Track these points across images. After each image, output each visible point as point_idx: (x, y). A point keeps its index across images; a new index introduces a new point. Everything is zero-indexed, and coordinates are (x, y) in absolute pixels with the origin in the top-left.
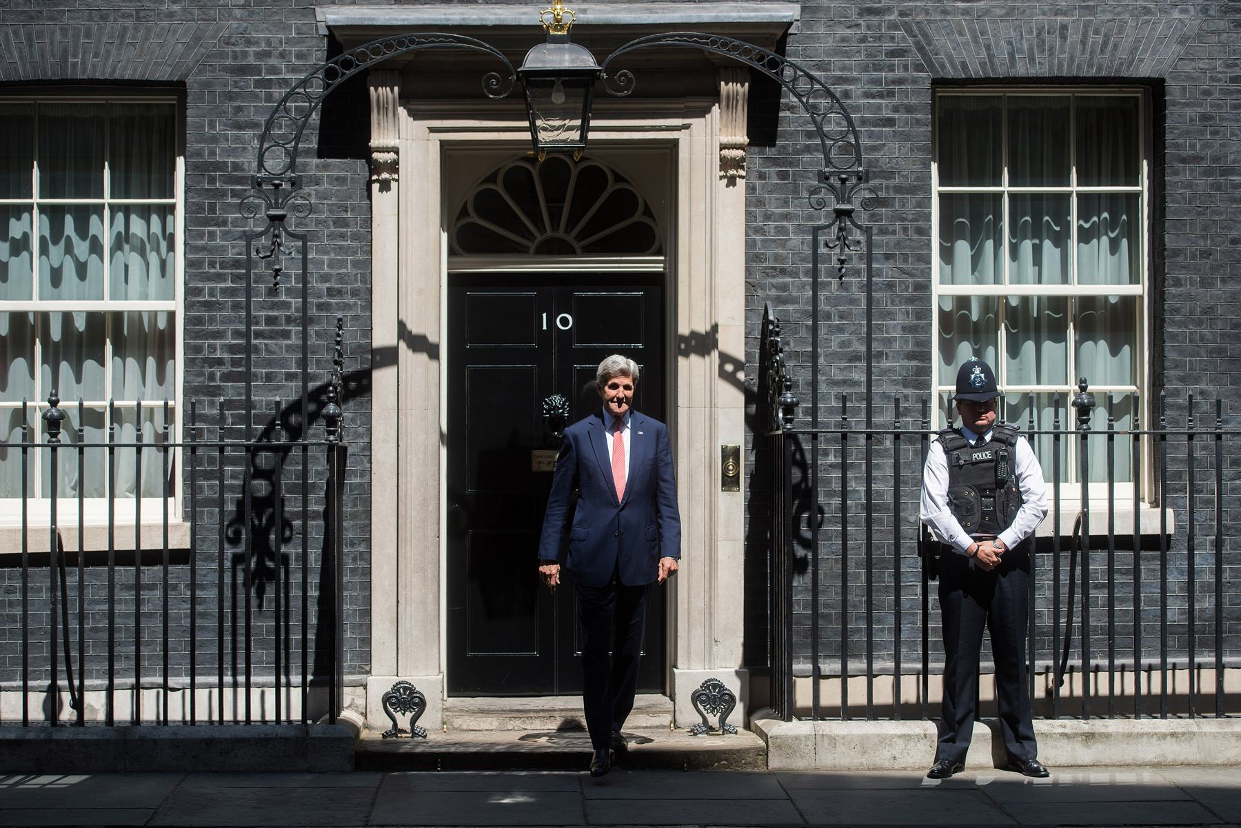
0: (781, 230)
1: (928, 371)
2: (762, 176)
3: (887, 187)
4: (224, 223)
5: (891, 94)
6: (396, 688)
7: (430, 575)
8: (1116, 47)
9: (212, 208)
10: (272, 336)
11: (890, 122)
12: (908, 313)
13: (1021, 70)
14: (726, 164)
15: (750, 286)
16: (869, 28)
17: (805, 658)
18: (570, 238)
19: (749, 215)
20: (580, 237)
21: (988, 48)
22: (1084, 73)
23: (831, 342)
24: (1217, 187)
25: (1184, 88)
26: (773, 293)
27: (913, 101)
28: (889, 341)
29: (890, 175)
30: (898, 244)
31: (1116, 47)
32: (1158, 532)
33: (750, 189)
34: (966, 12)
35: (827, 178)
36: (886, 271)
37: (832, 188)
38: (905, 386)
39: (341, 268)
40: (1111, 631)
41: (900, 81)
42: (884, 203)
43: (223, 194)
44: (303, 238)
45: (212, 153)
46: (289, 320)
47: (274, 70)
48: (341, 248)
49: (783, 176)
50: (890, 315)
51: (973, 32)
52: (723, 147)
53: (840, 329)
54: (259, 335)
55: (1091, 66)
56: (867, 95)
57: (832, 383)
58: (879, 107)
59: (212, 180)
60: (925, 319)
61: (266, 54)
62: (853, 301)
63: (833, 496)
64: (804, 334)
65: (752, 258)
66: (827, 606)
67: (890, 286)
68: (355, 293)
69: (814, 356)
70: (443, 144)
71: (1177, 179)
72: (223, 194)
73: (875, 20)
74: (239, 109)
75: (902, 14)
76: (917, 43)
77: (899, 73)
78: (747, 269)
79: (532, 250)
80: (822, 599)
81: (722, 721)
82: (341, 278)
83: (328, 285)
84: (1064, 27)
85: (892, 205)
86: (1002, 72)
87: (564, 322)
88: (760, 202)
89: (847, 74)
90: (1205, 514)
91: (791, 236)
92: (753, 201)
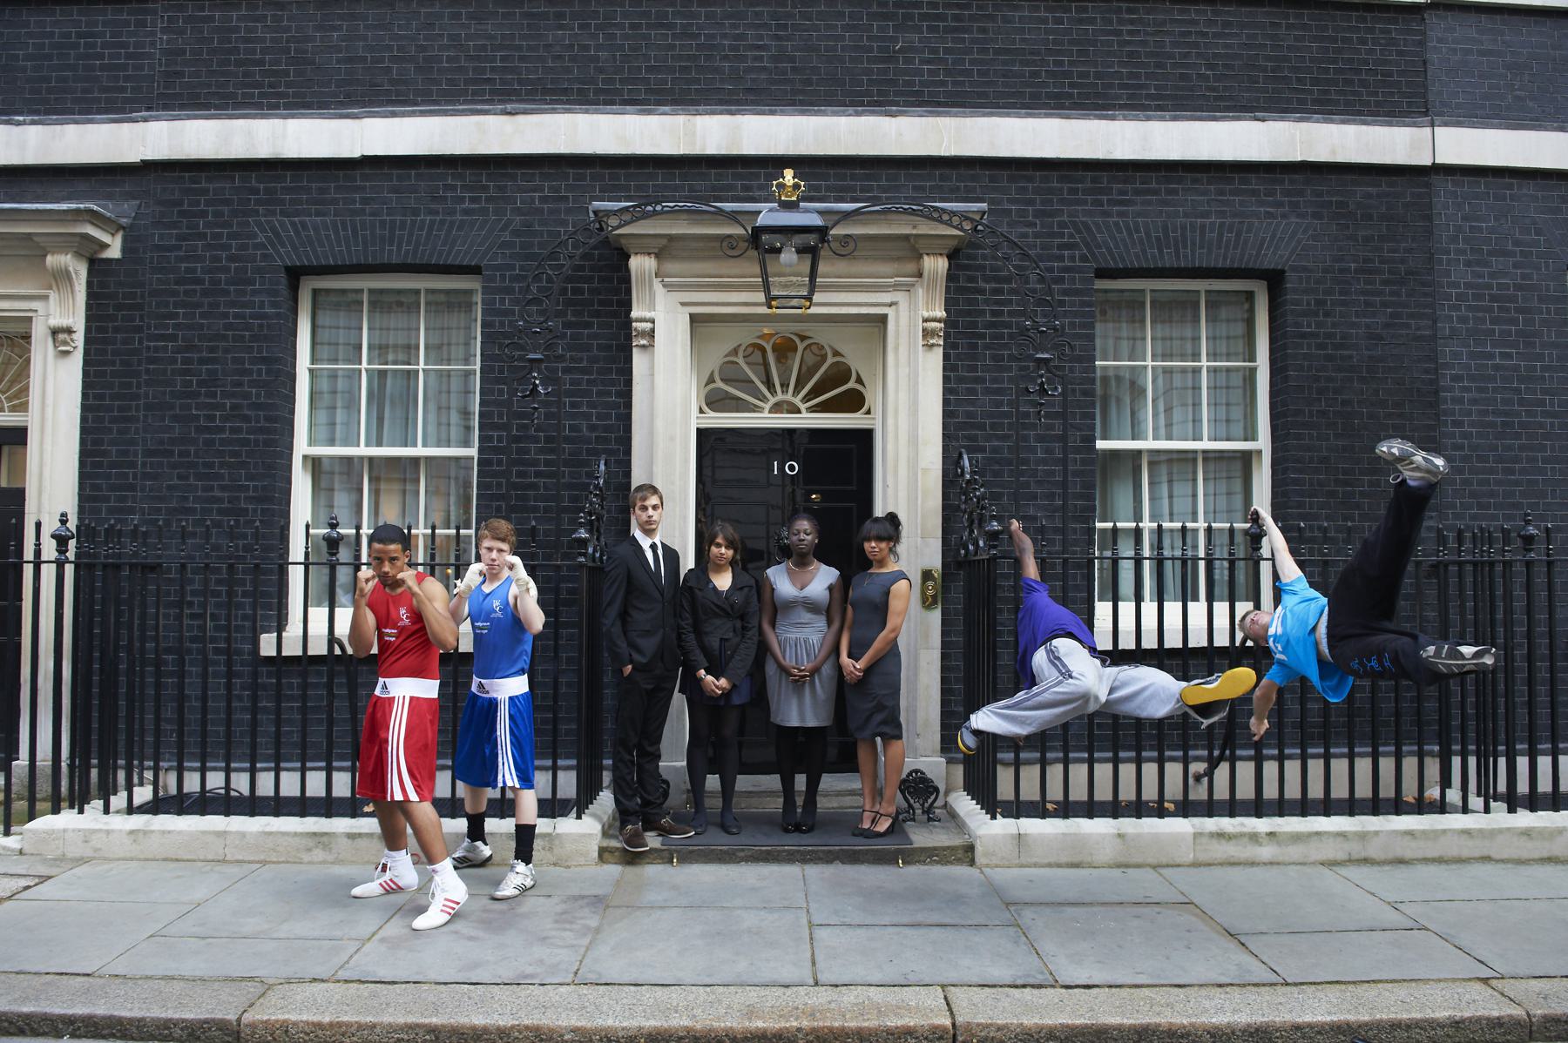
2: (955, 346)
14: (927, 333)
15: (946, 437)
16: (1042, 226)
18: (797, 401)
19: (946, 379)
20: (806, 399)
24: (1329, 358)
31: (1246, 242)
33: (946, 357)
52: (925, 320)
54: (538, 474)
55: (1225, 258)
65: (947, 414)
82: (607, 429)
84: (1203, 227)
87: (792, 468)
92: (947, 367)
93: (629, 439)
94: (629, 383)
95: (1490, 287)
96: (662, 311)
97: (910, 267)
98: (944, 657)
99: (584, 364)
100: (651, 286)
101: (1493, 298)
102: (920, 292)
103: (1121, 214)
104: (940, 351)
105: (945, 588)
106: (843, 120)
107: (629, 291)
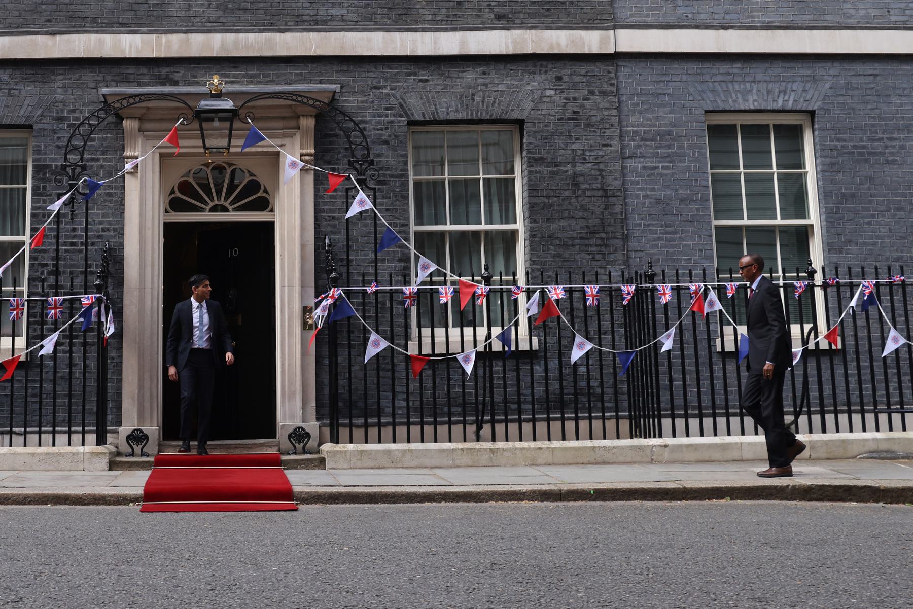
1: (409, 268)
4: (50, 195)
5: (387, 128)
8: (499, 104)
9: (44, 187)
10: (73, 252)
11: (387, 142)
13: (452, 116)
21: (435, 105)
22: (484, 117)
25: (534, 124)
26: (329, 228)
27: (399, 132)
29: (388, 169)
32: (528, 349)
34: (424, 88)
40: (505, 401)
41: (392, 122)
43: (49, 180)
45: (45, 160)
46: (82, 243)
47: (77, 119)
51: (427, 97)
53: (363, 247)
54: (66, 251)
56: (374, 129)
57: (358, 274)
58: (381, 135)
59: (45, 174)
61: (73, 111)
68: (115, 230)
69: (349, 261)
70: (162, 155)
71: (532, 169)
72: (49, 180)
73: (377, 92)
74: (59, 138)
75: (391, 89)
76: (400, 103)
77: (392, 118)
82: (110, 223)
86: (442, 118)
88: (322, 183)
89: (364, 119)
90: (552, 340)
95: (655, 125)
101: (658, 133)
103: (424, 88)
106: (251, 36)
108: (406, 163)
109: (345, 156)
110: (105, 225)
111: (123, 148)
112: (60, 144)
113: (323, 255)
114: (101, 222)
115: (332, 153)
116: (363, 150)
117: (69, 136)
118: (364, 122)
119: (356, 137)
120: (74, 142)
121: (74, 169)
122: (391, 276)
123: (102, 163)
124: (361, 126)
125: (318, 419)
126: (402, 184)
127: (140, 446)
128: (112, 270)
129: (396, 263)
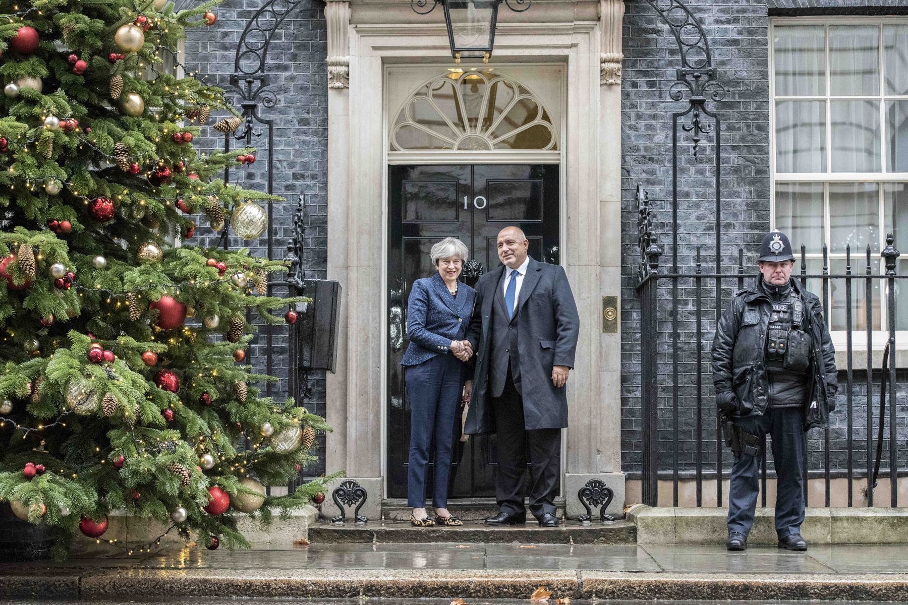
0: (649, 127)
2: (635, 85)
3: (734, 94)
5: (736, 20)
6: (344, 484)
7: (370, 396)
12: (751, 192)
15: (626, 171)
17: (670, 465)
23: (688, 218)
28: (735, 215)
30: (742, 139)
33: (625, 95)
35: (684, 75)
36: (732, 159)
37: (689, 84)
38: (749, 250)
39: (303, 157)
41: (744, 11)
42: (731, 106)
44: (269, 123)
45: (204, 68)
48: (304, 142)
49: (651, 84)
50: (736, 194)
53: (697, 205)
56: (717, 22)
57: (689, 246)
58: (726, 31)
60: (764, 197)
62: (706, 184)
63: (692, 337)
64: (669, 208)
65: (627, 149)
66: (687, 424)
67: (736, 171)
68: (314, 177)
69: (675, 226)
70: (385, 61)
74: (225, 35)
77: (744, 4)
78: (623, 158)
79: (456, 147)
80: (682, 419)
81: (603, 510)
82: (305, 165)
83: (293, 170)
85: (738, 108)
87: (480, 203)
88: (634, 106)
91: (658, 132)
93: (325, 175)
94: (325, 121)
96: (355, 54)
97: (590, 11)
98: (624, 379)
99: (282, 105)
100: (345, 33)
102: (598, 34)
104: (619, 89)
105: (625, 316)
107: (324, 36)
108: (765, 75)
109: (670, 63)
110: (297, 170)
111: (325, 48)
112: (227, 41)
113: (635, 219)
114: (292, 165)
115: (649, 59)
116: (698, 53)
117: (241, 31)
118: (700, 10)
119: (690, 36)
120: (249, 40)
121: (250, 83)
122: (741, 251)
123: (291, 72)
124: (698, 15)
125: (624, 468)
126: (758, 107)
127: (354, 507)
128: (310, 237)
129: (746, 231)
